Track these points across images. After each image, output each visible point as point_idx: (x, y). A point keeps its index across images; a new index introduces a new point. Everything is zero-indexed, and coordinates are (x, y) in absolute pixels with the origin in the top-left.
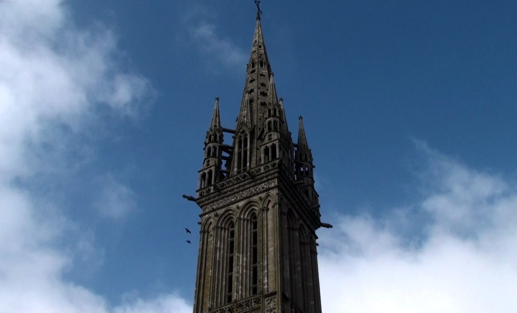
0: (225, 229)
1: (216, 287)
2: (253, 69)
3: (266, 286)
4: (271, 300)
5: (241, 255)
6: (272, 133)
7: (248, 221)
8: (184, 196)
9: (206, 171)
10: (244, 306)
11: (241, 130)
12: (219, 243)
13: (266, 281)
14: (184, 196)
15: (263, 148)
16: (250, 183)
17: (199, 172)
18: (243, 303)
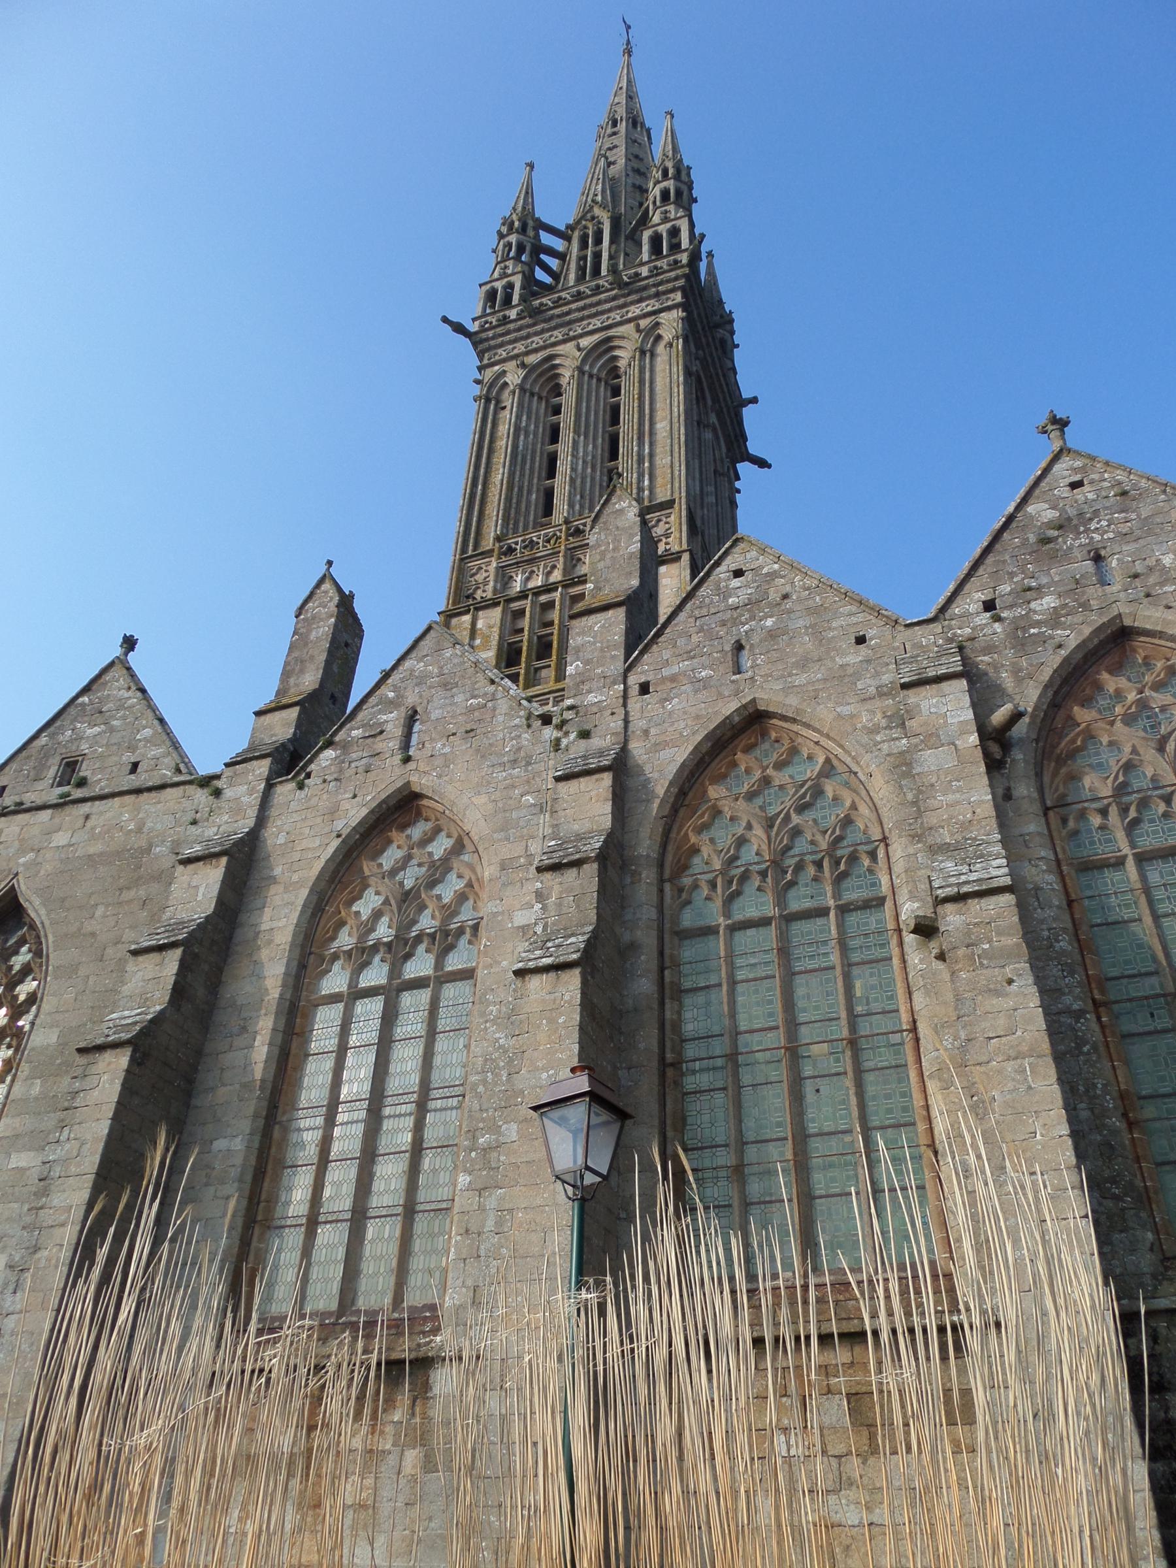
0: (540, 398)
1: (514, 501)
2: (615, 129)
3: (647, 493)
5: (582, 438)
6: (671, 208)
7: (599, 380)
8: (445, 320)
9: (499, 285)
11: (589, 216)
12: (524, 418)
13: (646, 483)
14: (445, 320)
15: (646, 235)
16: (614, 298)
17: (481, 285)
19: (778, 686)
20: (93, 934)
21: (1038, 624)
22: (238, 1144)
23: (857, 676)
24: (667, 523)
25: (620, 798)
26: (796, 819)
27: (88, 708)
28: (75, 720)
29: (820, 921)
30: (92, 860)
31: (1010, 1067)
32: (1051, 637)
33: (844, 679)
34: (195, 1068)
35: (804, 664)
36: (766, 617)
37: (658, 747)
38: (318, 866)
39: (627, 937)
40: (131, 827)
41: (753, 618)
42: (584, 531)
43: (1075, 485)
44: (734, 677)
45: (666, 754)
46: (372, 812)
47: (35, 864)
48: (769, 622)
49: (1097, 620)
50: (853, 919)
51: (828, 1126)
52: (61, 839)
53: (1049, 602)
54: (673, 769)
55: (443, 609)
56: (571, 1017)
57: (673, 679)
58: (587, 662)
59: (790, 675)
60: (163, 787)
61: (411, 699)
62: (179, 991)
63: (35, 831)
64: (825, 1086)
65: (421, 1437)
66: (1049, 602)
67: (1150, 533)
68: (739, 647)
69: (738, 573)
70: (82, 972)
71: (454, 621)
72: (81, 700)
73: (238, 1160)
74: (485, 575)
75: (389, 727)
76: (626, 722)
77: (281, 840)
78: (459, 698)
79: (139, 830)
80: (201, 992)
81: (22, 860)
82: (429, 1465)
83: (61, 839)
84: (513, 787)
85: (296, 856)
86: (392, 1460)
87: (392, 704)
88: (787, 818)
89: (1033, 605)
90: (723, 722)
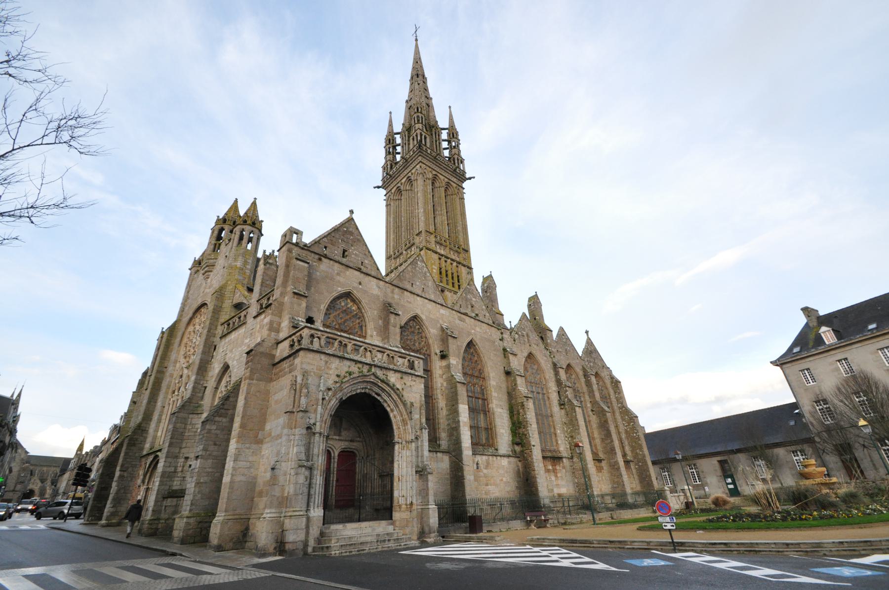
68: (566, 350)
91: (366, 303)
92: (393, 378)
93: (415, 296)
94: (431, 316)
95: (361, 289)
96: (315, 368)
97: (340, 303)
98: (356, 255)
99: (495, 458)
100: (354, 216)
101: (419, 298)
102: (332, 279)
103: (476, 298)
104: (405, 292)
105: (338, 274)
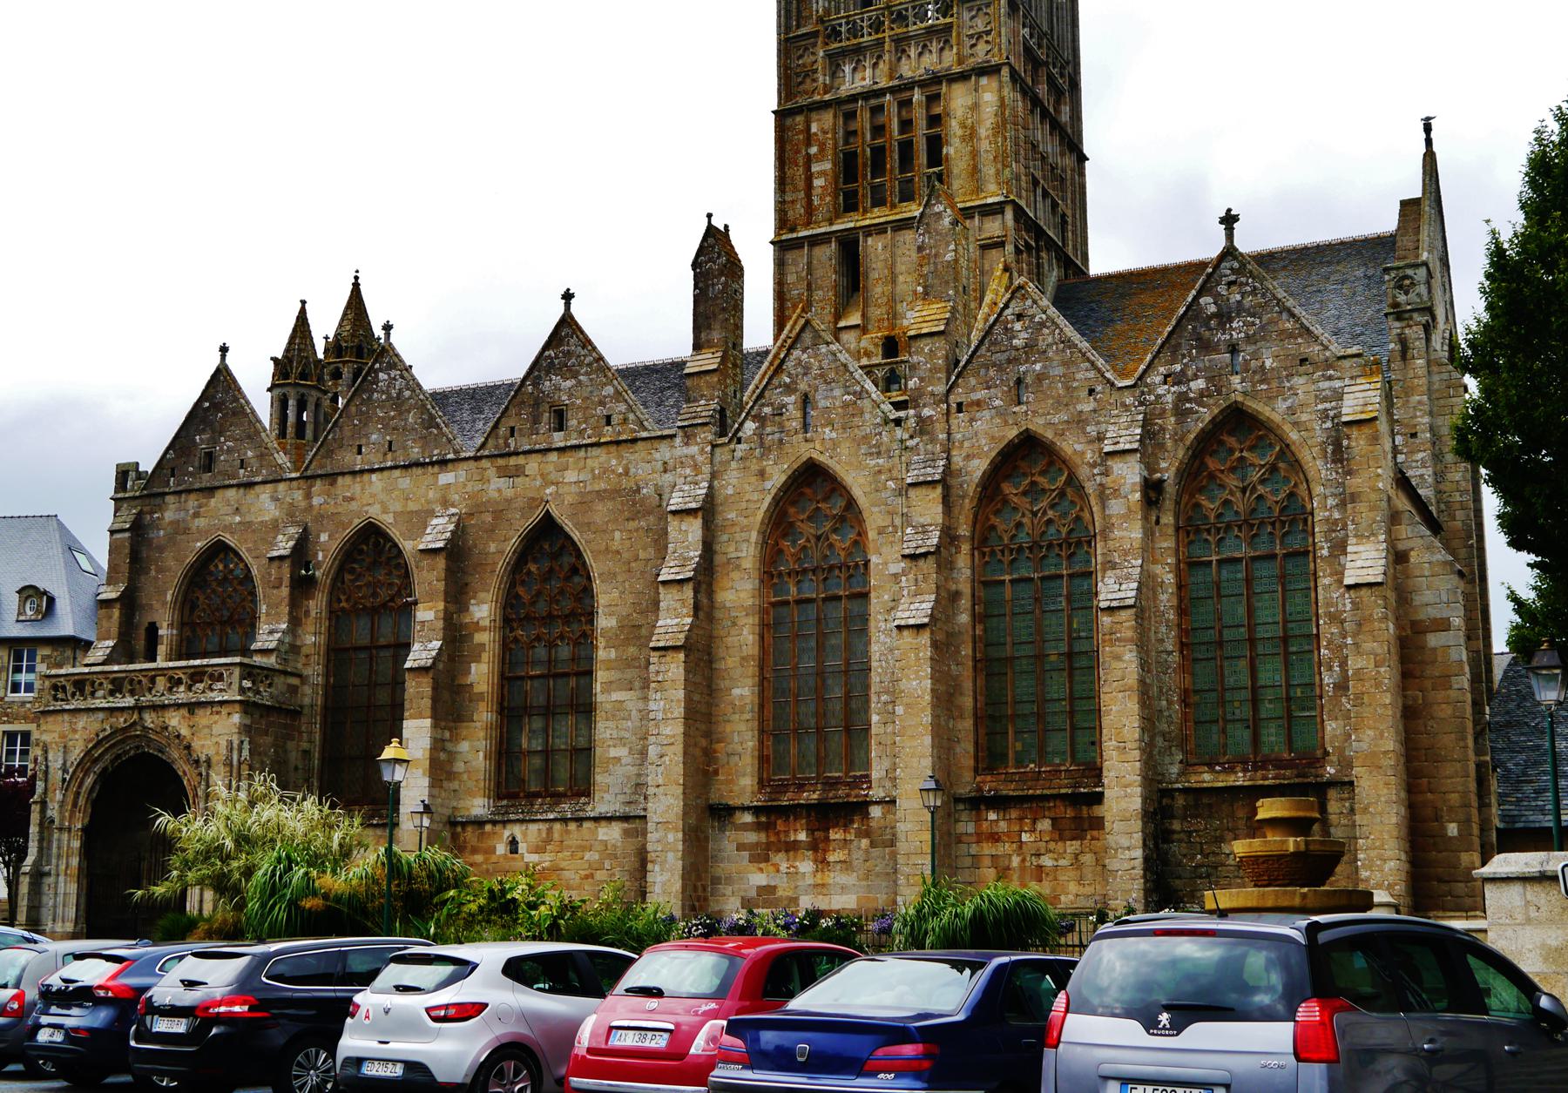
4: (979, 9)
10: (911, 19)
18: (907, 10)
19: (1041, 421)
20: (618, 552)
21: (1189, 400)
22: (746, 692)
23: (1086, 422)
24: (986, 14)
25: (946, 501)
26: (1050, 514)
27: (556, 361)
28: (548, 372)
29: (1059, 582)
30: (600, 495)
31: (1121, 695)
32: (1197, 412)
33: (1080, 421)
34: (709, 646)
35: (1059, 404)
36: (1034, 363)
37: (968, 457)
38: (760, 515)
39: (954, 587)
40: (621, 470)
41: (1026, 362)
42: (906, 18)
43: (1230, 284)
44: (1016, 409)
45: (976, 462)
46: (789, 477)
47: (557, 494)
48: (1038, 367)
49: (1223, 404)
50: (1076, 581)
51: (1055, 696)
52: (571, 476)
53: (1200, 384)
54: (979, 473)
55: (776, 108)
56: (928, 653)
57: (978, 403)
58: (921, 379)
59: (1049, 414)
60: (634, 441)
61: (803, 386)
62: (697, 608)
63: (551, 468)
64: (1055, 674)
65: (867, 834)
66: (1200, 384)
67: (1263, 338)
68: (1019, 382)
69: (1019, 317)
70: (620, 578)
71: (789, 122)
72: (547, 353)
73: (748, 701)
74: (812, 58)
75: (790, 407)
76: (949, 434)
77: (730, 491)
78: (837, 392)
79: (627, 473)
80: (705, 601)
81: (548, 491)
82: (873, 845)
83: (571, 476)
84: (880, 472)
85: (744, 505)
86: (855, 843)
87: (789, 389)
88: (1045, 513)
89: (1192, 384)
90: (1008, 444)
91: (249, 550)
92: (175, 720)
93: (366, 477)
94: (412, 506)
95: (240, 523)
96: (56, 735)
97: (216, 566)
98: (230, 450)
99: (572, 826)
100: (230, 360)
101: (374, 477)
102: (186, 531)
103: (575, 375)
104: (340, 480)
105: (196, 515)
